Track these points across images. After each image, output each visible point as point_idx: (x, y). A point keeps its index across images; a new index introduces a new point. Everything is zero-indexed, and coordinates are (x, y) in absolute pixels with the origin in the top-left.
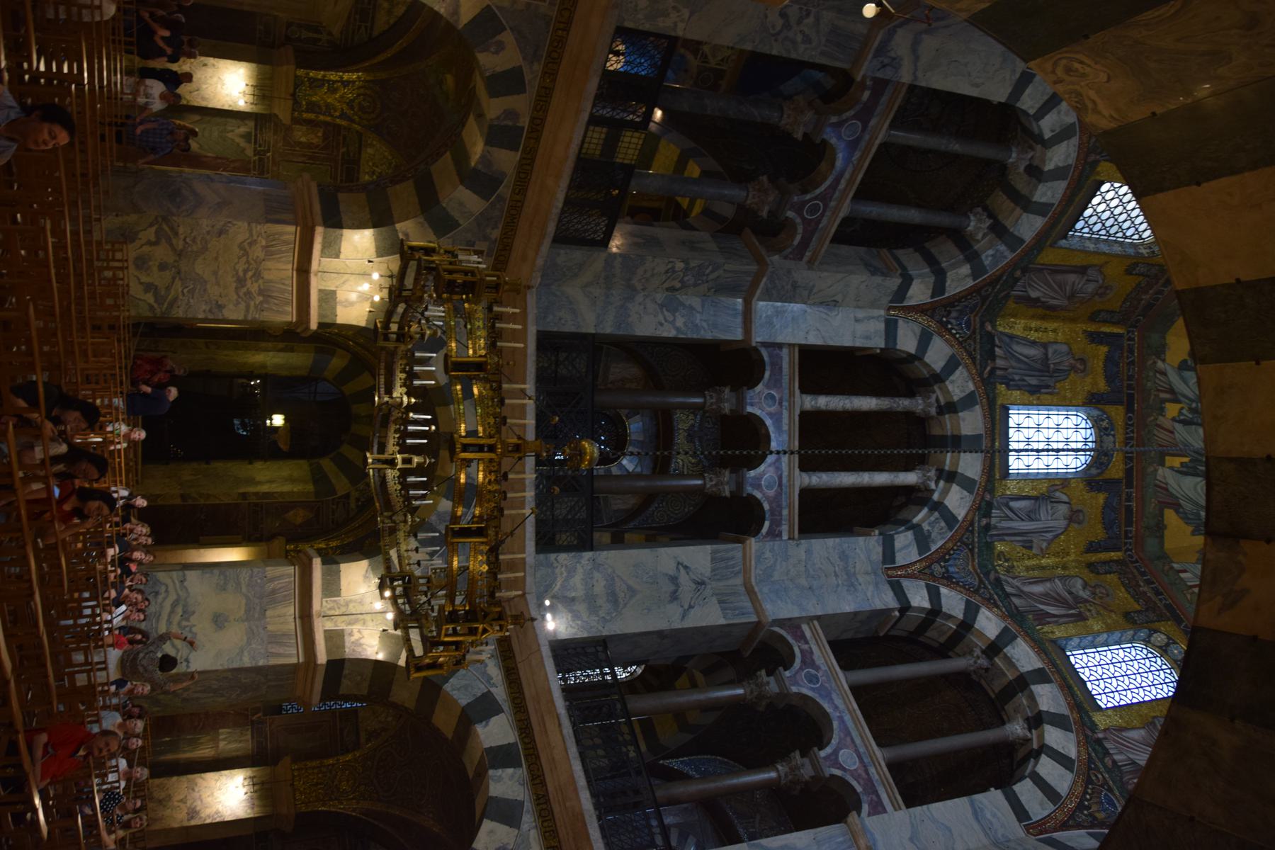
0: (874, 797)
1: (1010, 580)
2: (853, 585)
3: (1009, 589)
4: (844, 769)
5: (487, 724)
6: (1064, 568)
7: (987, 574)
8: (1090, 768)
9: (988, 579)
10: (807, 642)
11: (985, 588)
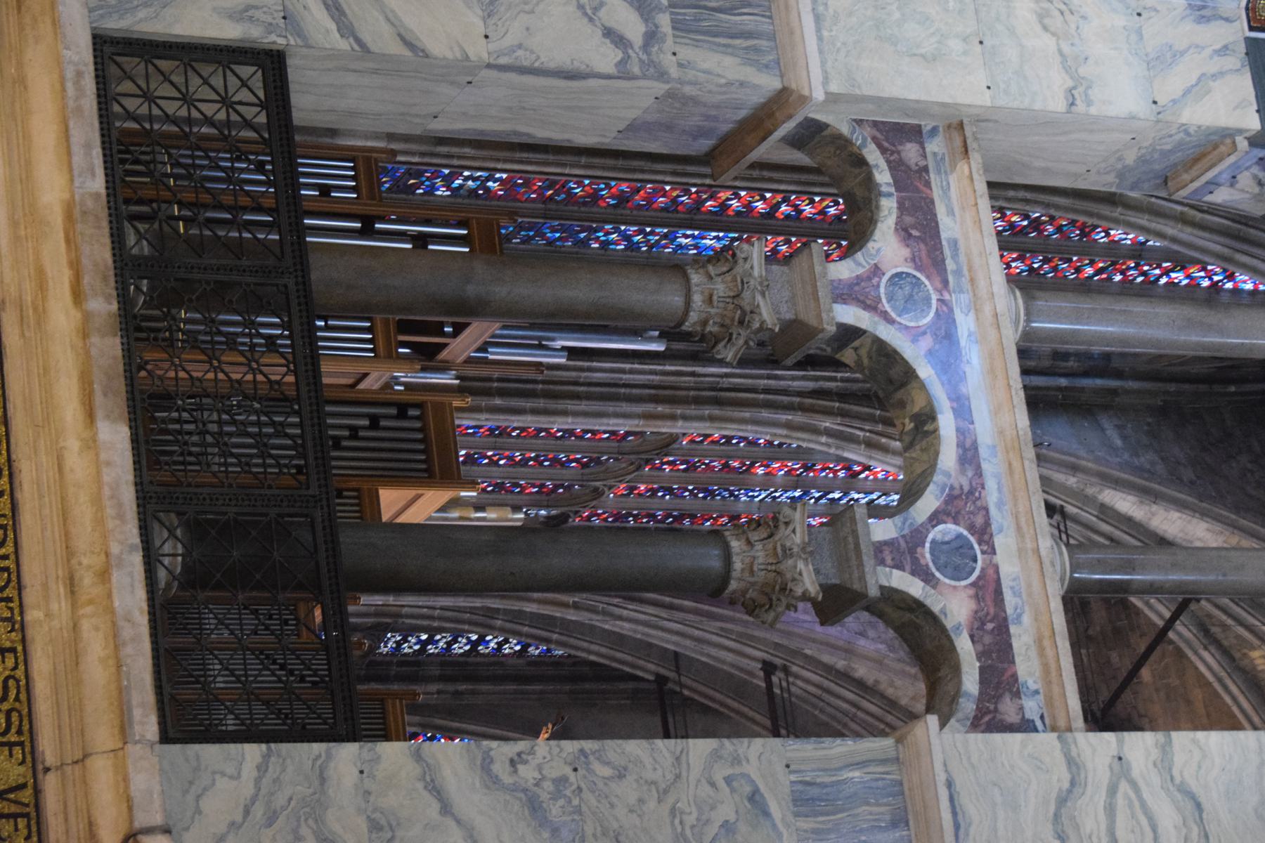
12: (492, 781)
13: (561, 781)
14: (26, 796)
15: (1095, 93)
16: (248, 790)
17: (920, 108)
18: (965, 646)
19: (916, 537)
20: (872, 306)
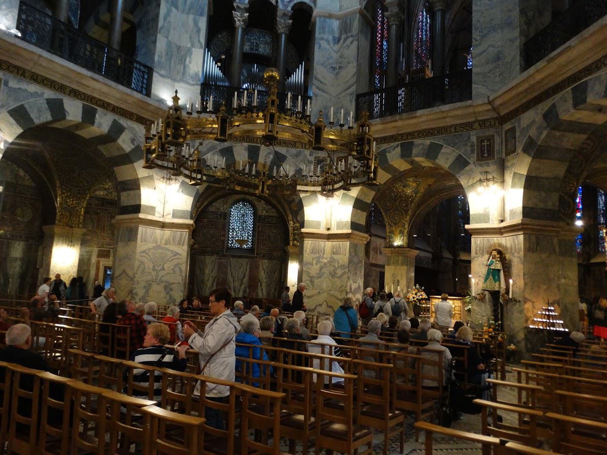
5: (67, 112)
12: (480, 44)
13: (480, 32)
14: (481, 123)
16: (480, 86)
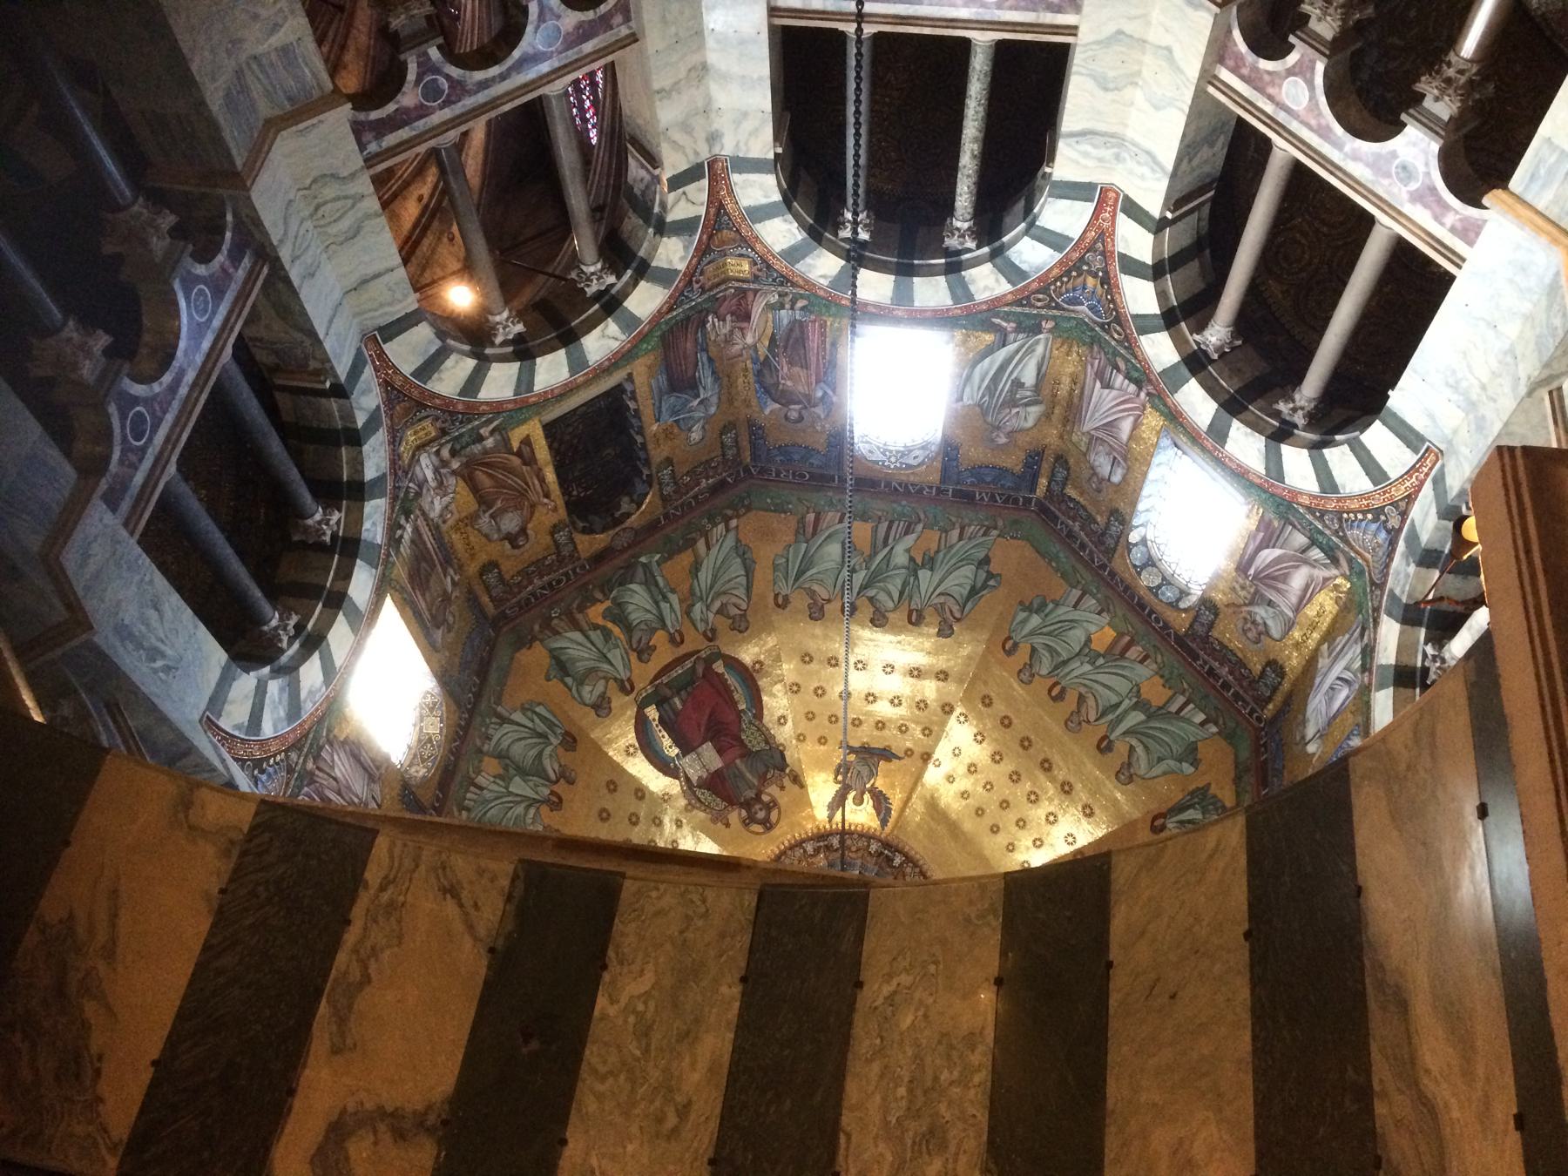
0: (1245, 71)
1: (1327, 573)
2: (1455, 387)
3: (1316, 554)
4: (1290, 72)
6: (1297, 645)
7: (1350, 561)
8: (1127, 338)
9: (1343, 551)
10: (1453, 230)
11: (1336, 533)
15: (665, 102)
17: (639, 18)
18: (391, 108)
19: (437, 70)
20: (542, 18)
